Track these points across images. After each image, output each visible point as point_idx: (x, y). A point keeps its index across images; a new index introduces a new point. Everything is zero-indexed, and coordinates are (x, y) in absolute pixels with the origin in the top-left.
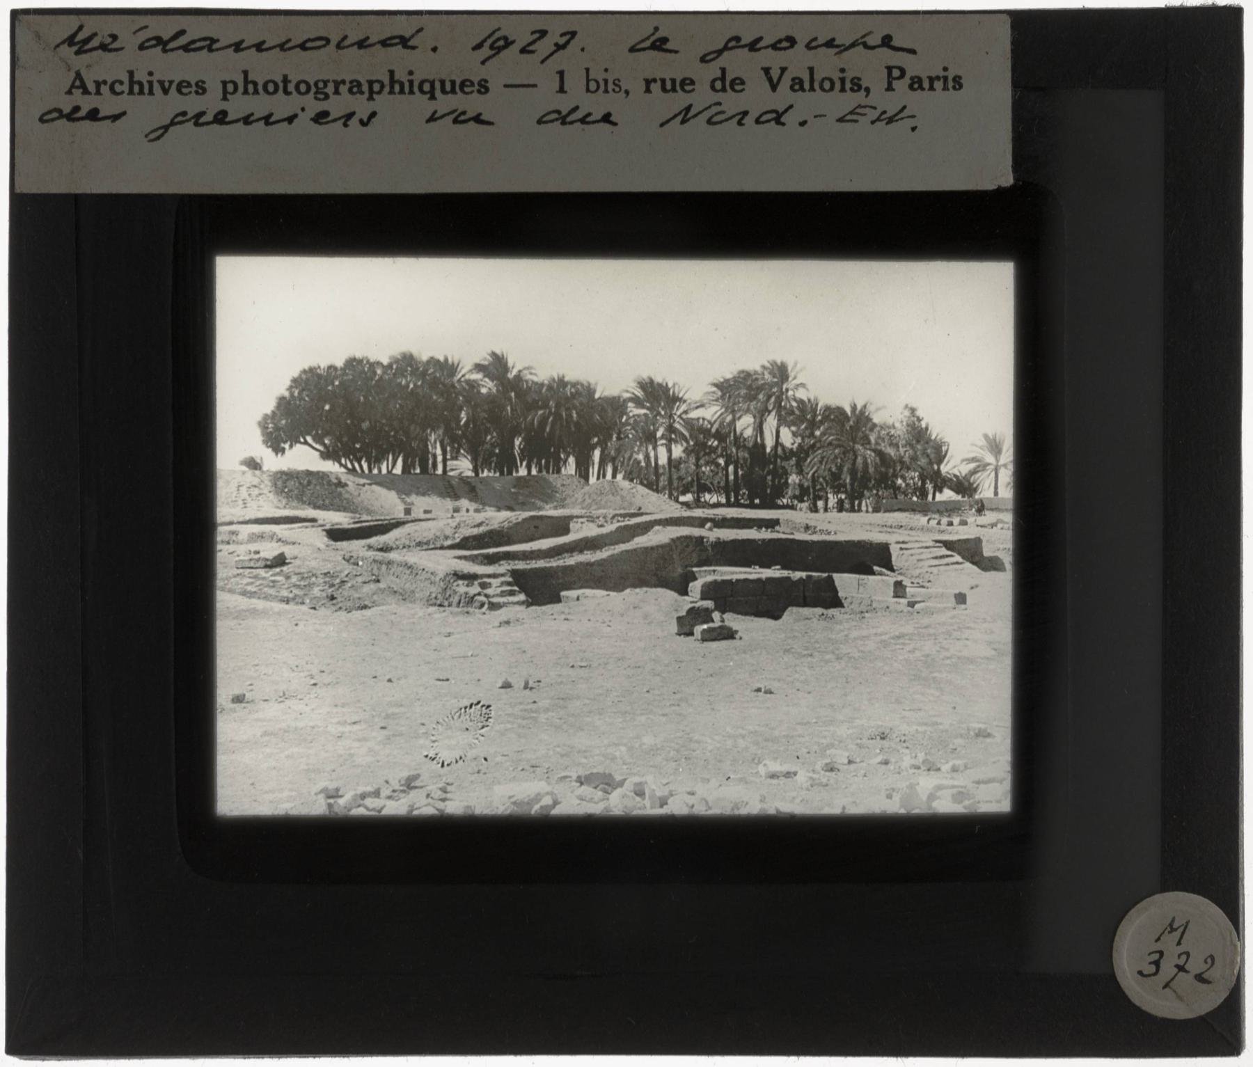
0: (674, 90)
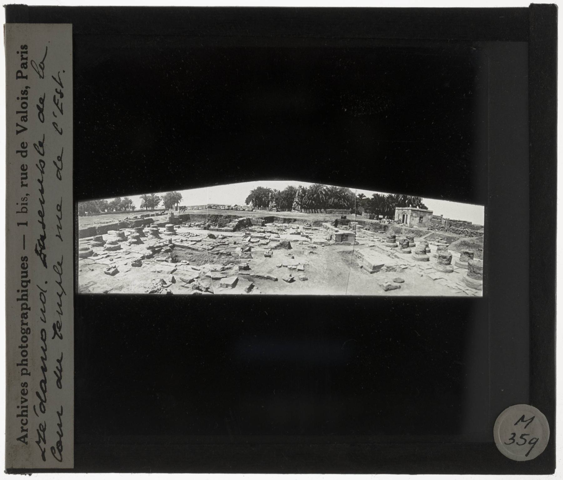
0: (26, 174)
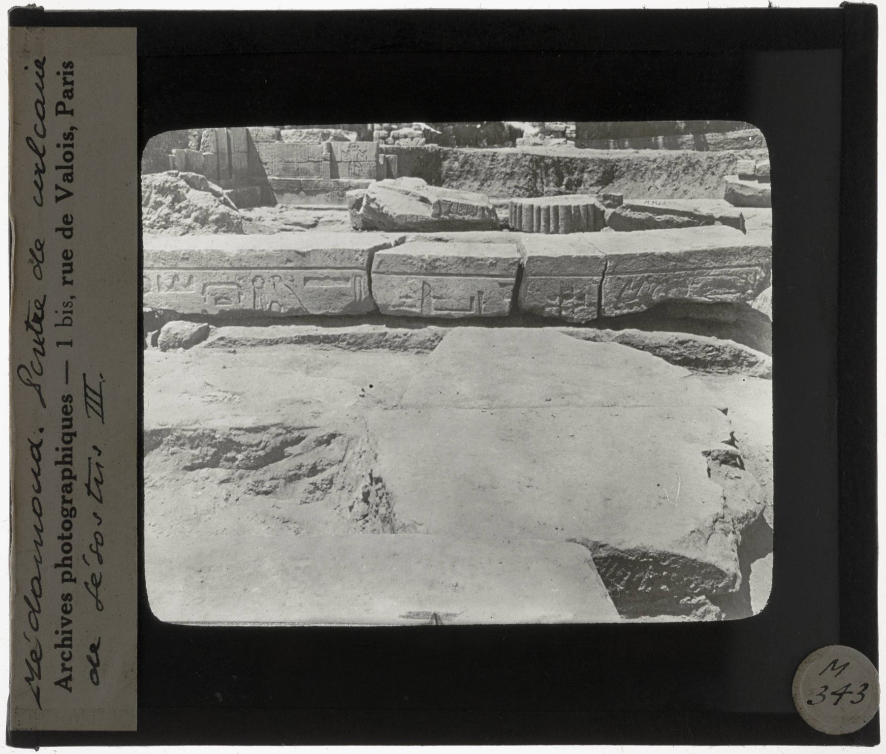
0: (71, 265)
